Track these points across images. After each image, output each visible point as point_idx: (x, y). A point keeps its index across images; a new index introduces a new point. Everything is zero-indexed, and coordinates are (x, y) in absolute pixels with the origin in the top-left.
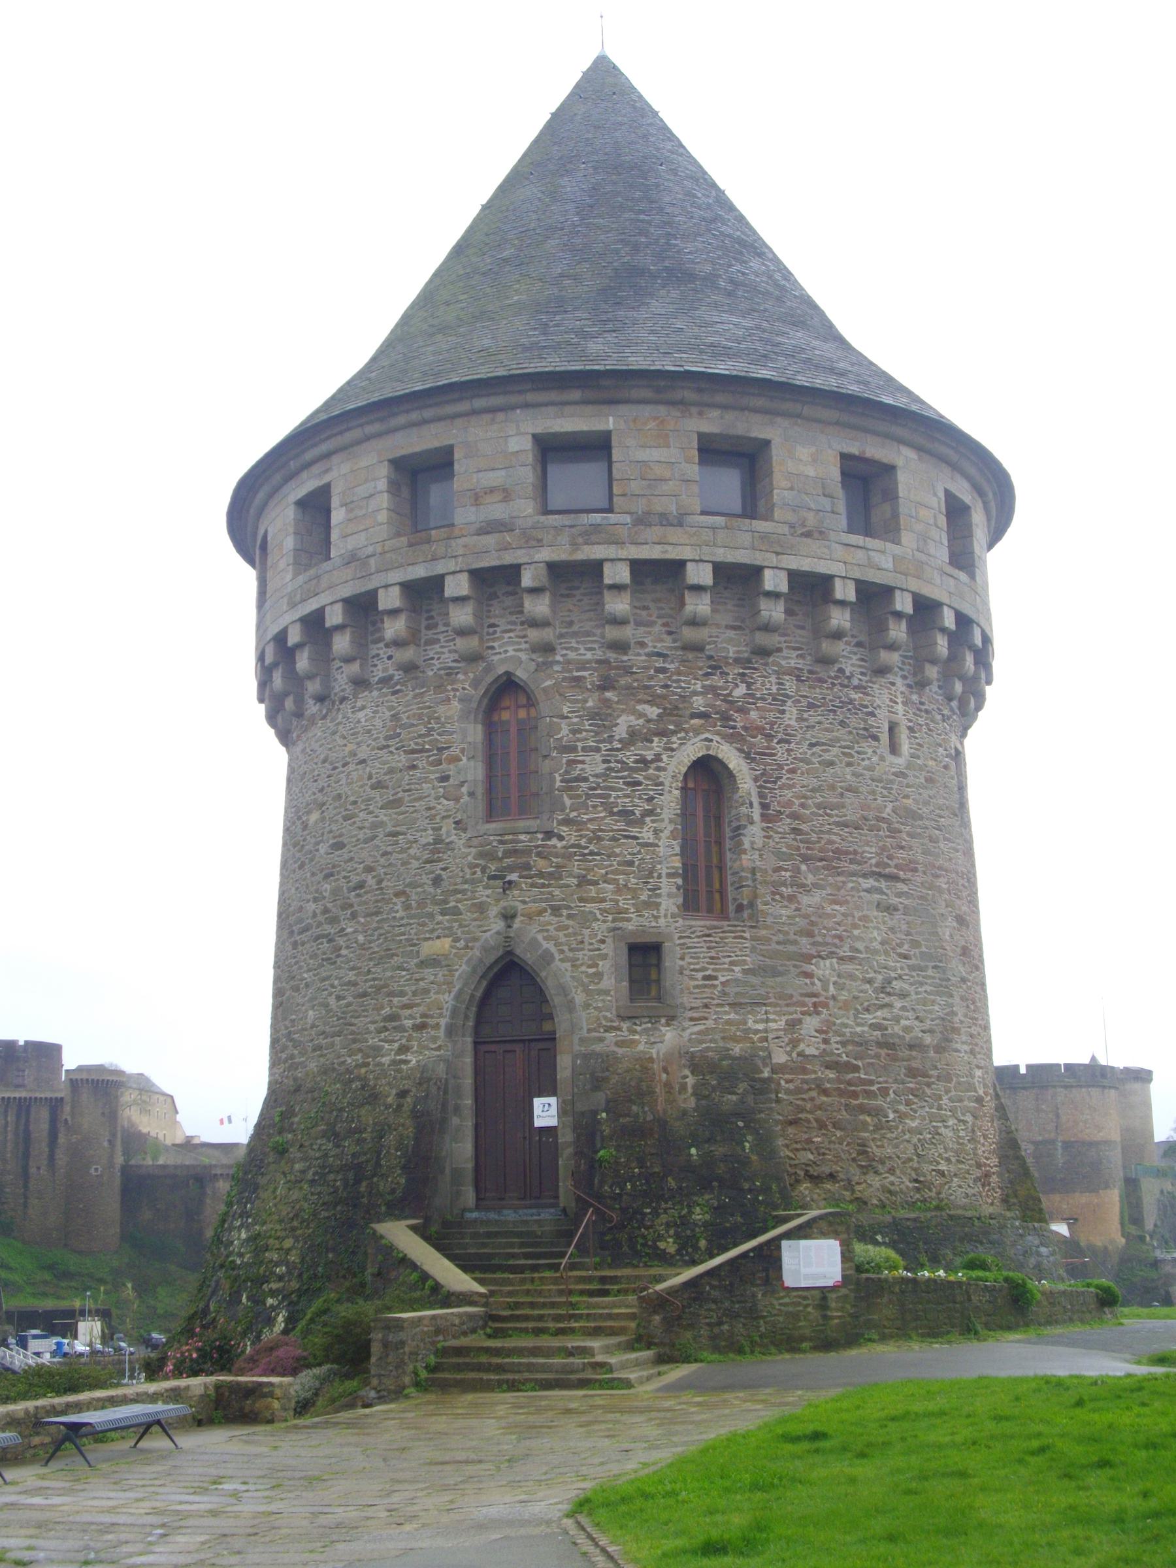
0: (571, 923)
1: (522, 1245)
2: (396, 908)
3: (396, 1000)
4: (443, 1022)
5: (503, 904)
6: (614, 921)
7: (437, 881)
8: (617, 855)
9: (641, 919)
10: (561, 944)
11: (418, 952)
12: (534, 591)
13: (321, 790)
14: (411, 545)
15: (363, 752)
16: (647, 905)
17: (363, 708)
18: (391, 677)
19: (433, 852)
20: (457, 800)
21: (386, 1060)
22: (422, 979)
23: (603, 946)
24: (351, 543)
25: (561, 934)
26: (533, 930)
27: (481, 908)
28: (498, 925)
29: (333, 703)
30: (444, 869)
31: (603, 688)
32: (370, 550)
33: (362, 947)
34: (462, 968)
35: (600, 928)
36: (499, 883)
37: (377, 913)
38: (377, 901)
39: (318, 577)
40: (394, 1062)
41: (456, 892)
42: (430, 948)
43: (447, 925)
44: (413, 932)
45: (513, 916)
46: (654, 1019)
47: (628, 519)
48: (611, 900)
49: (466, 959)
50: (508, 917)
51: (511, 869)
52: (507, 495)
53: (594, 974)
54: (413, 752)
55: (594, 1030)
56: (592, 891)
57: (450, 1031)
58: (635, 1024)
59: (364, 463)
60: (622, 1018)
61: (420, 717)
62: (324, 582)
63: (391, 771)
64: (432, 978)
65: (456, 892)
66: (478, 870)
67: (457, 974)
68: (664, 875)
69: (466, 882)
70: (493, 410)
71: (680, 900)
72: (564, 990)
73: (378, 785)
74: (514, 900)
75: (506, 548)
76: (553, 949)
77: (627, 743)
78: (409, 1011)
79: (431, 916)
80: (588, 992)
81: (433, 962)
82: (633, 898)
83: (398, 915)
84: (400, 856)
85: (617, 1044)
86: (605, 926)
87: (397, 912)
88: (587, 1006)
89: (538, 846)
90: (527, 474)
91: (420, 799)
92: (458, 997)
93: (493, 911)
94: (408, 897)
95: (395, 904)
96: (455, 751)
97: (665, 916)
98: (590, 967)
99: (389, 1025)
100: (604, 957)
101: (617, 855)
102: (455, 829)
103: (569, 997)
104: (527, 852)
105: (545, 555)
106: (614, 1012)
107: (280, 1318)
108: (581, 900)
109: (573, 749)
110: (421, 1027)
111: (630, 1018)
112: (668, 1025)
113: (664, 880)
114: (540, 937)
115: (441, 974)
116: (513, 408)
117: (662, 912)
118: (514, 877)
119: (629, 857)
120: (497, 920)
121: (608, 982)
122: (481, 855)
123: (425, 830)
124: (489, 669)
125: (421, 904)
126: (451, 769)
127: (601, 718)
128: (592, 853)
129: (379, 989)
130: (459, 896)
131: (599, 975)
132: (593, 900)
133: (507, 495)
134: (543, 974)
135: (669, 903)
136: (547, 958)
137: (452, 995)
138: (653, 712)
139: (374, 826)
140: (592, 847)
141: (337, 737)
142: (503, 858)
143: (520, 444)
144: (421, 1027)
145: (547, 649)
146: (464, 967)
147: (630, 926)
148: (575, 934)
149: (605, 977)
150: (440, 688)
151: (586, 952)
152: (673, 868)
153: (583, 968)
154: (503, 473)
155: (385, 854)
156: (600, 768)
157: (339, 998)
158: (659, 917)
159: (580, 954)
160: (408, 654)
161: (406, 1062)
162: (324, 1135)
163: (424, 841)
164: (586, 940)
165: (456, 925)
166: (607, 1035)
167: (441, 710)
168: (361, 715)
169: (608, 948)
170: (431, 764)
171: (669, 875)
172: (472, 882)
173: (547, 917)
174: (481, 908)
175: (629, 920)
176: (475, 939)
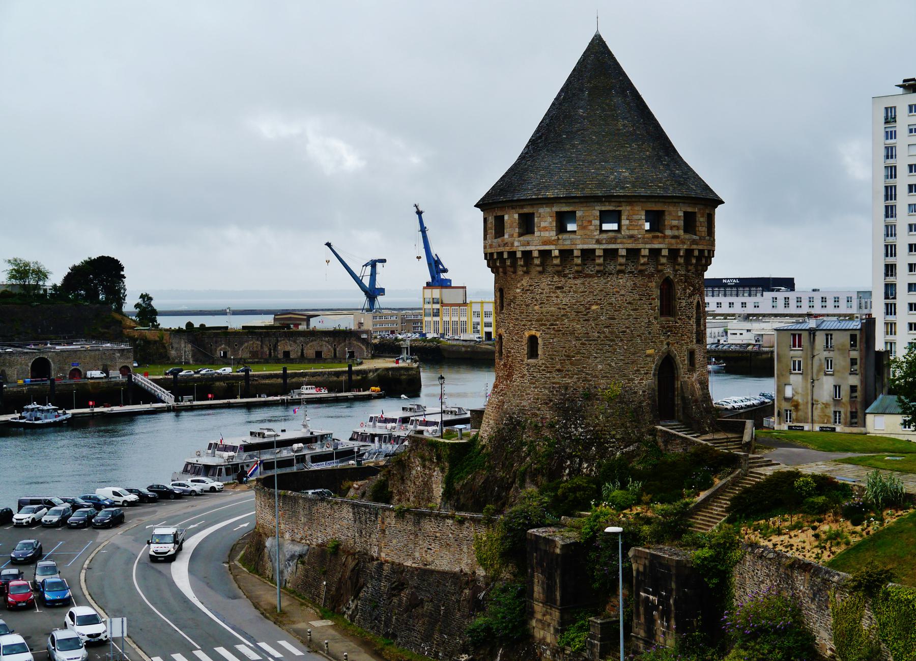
4: (652, 372)
7: (650, 333)
12: (681, 256)
13: (601, 299)
15: (622, 292)
17: (621, 279)
18: (634, 272)
19: (648, 325)
20: (655, 311)
24: (631, 232)
26: (673, 348)
27: (662, 342)
29: (605, 274)
31: (685, 282)
32: (640, 236)
33: (626, 350)
37: (631, 341)
40: (639, 383)
42: (649, 352)
47: (697, 238)
50: (668, 344)
51: (668, 331)
52: (678, 228)
54: (641, 295)
57: (654, 375)
59: (636, 208)
60: (688, 371)
61: (643, 285)
62: (619, 241)
63: (634, 300)
65: (655, 337)
70: (675, 203)
74: (670, 340)
75: (677, 243)
77: (689, 297)
79: (649, 343)
80: (683, 365)
90: (682, 223)
91: (644, 309)
92: (656, 366)
93: (665, 343)
94: (641, 337)
96: (654, 296)
99: (637, 372)
100: (685, 355)
104: (671, 327)
105: (685, 247)
107: (618, 453)
109: (680, 299)
110: (646, 374)
116: (679, 203)
118: (669, 333)
121: (686, 362)
122: (661, 327)
124: (664, 274)
125: (645, 340)
127: (684, 290)
129: (633, 363)
131: (684, 360)
133: (678, 228)
138: (692, 288)
139: (628, 315)
141: (608, 285)
143: (681, 214)
144: (646, 374)
145: (677, 271)
147: (689, 347)
150: (649, 278)
154: (677, 222)
155: (633, 324)
156: (684, 305)
157: (616, 364)
160: (643, 268)
162: (620, 403)
167: (650, 284)
168: (621, 280)
169: (686, 353)
170: (647, 299)
173: (676, 345)
174: (662, 342)
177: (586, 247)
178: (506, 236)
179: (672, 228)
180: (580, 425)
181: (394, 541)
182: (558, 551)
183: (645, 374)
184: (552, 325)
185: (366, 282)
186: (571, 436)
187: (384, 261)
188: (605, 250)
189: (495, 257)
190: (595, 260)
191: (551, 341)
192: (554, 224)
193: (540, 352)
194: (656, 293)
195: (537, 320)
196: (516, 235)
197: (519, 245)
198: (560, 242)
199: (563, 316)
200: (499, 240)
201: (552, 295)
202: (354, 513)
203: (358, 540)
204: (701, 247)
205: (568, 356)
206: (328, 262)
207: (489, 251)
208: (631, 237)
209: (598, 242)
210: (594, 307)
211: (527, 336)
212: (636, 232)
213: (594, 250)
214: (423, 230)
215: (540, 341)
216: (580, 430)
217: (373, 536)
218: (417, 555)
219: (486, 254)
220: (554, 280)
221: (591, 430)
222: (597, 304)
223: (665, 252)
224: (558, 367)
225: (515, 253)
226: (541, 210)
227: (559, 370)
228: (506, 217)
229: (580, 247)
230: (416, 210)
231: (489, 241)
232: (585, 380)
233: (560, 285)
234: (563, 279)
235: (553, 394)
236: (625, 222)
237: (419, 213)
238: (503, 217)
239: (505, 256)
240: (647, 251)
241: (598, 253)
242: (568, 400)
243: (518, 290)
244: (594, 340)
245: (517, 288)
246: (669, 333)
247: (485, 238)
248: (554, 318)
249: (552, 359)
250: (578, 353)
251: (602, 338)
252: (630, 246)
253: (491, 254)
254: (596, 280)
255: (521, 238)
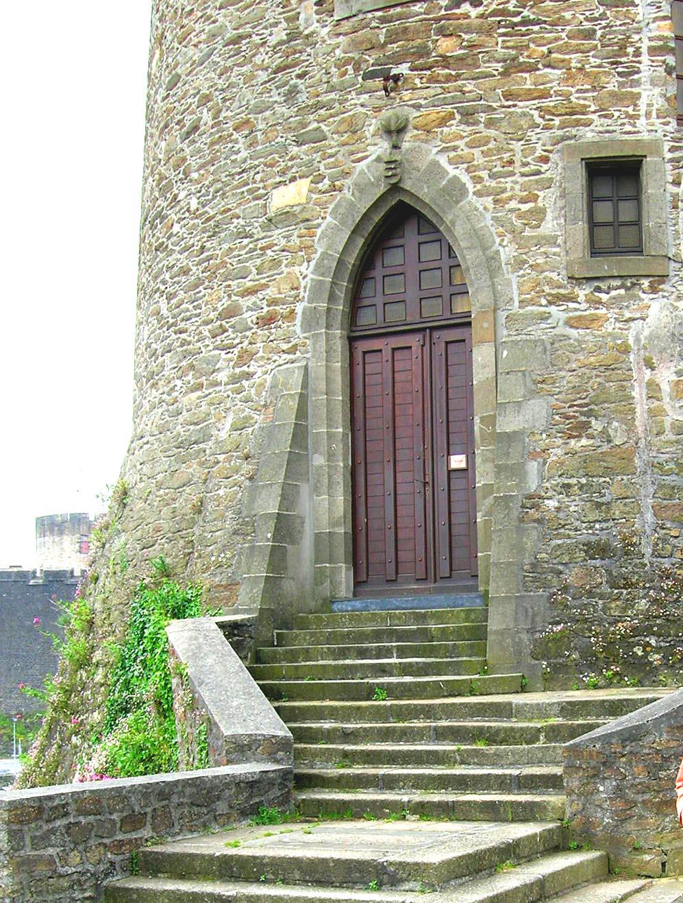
0: (492, 133)
1: (402, 653)
2: (237, 146)
3: (233, 283)
4: (299, 308)
5: (385, 113)
6: (561, 128)
7: (292, 94)
8: (567, 23)
9: (609, 121)
10: (477, 168)
11: (265, 206)
16: (617, 98)
21: (222, 376)
22: (269, 247)
23: (545, 167)
25: (477, 152)
26: (432, 152)
28: (381, 147)
30: (300, 76)
35: (541, 140)
36: (378, 82)
38: (213, 144)
40: (235, 379)
41: (318, 106)
43: (306, 158)
44: (258, 177)
45: (401, 130)
46: (630, 281)
48: (557, 94)
49: (331, 206)
50: (395, 131)
53: (530, 211)
55: (532, 302)
56: (528, 81)
58: (598, 289)
64: (283, 242)
66: (350, 67)
67: (319, 231)
68: (644, 50)
69: (332, 89)
71: (672, 91)
72: (482, 243)
76: (465, 178)
78: (253, 299)
81: (287, 217)
82: (594, 89)
83: (239, 157)
84: (244, 69)
85: (569, 323)
86: (547, 134)
87: (239, 152)
88: (519, 264)
89: (438, 20)
95: (236, 141)
97: (648, 115)
98: (523, 201)
100: (548, 184)
101: (567, 23)
102: (317, 13)
103: (490, 253)
106: (564, 272)
108: (508, 96)
110: (267, 321)
111: (589, 279)
112: (654, 290)
113: (645, 58)
114: (443, 160)
117: (643, 109)
118: (403, 69)
119: (587, 25)
120: (378, 140)
122: (355, 45)
123: (276, 24)
128: (525, 22)
130: (322, 112)
131: (540, 214)
132: (529, 95)
134: (448, 218)
136: (455, 190)
137: (313, 264)
140: (526, 13)
142: (386, 44)
144: (267, 321)
146: (329, 219)
147: (589, 135)
148: (499, 150)
149: (549, 216)
151: (517, 178)
152: (660, 38)
153: (513, 204)
158: (637, 117)
159: (508, 182)
161: (249, 376)
163: (273, 41)
164: (518, 158)
165: (317, 156)
166: (553, 309)
171: (653, 51)
172: (342, 88)
173: (454, 127)
174: (354, 128)
175: (588, 124)
176: (346, 174)
246: (403, 69)
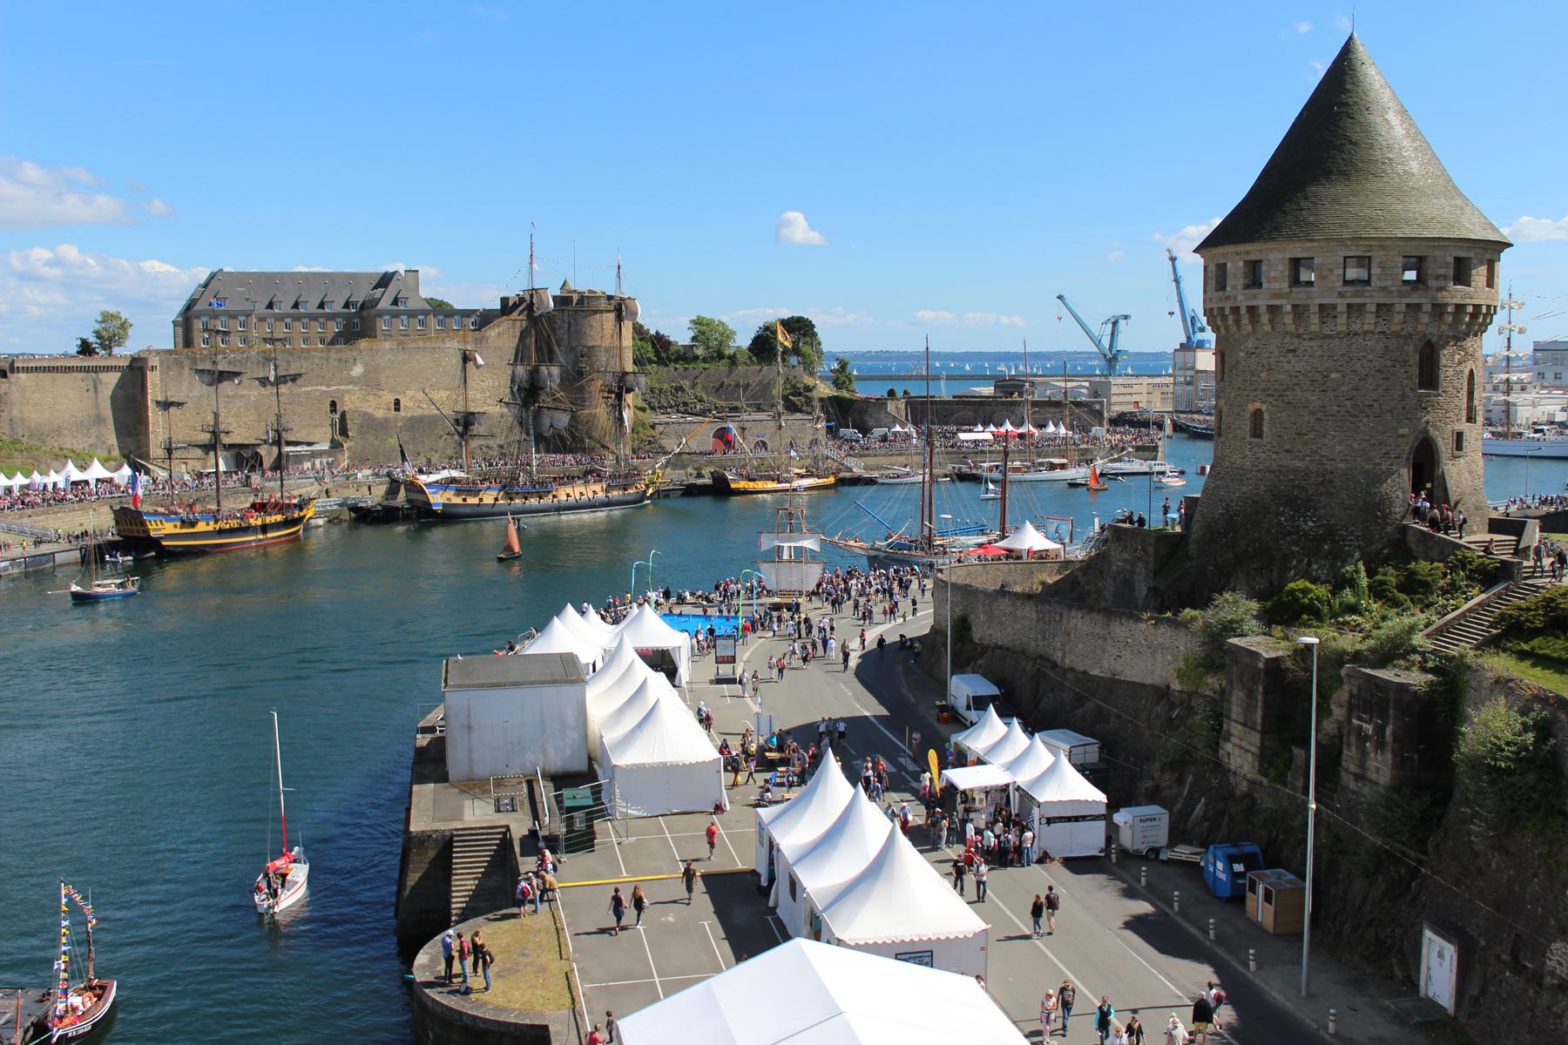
7: (1404, 408)
14: (1412, 290)
15: (1370, 357)
21: (1384, 467)
24: (1384, 284)
32: (1394, 288)
34: (1412, 439)
39: (1363, 291)
42: (1401, 431)
56: (1448, 415)
57: (1408, 459)
62: (1367, 294)
63: (1385, 366)
73: (1379, 371)
81: (1403, 436)
90: (1451, 272)
96: (1411, 363)
115: (1405, 440)
126: (1409, 369)
129: (1380, 443)
135: (1464, 419)
139: (1377, 385)
143: (1451, 260)
167: (1406, 348)
168: (1368, 343)
177: (1324, 301)
178: (1228, 289)
179: (1437, 277)
180: (1311, 517)
181: (1080, 646)
182: (1261, 665)
183: (1396, 458)
184: (1281, 395)
185: (1106, 342)
186: (1298, 532)
187: (1126, 317)
188: (1349, 306)
189: (1215, 313)
190: (1335, 317)
191: (1279, 415)
192: (1287, 273)
193: (1265, 429)
194: (1415, 358)
195: (1263, 390)
196: (1240, 287)
197: (1243, 301)
198: (1294, 295)
199: (1295, 385)
200: (1221, 293)
201: (1282, 359)
202: (1037, 612)
203: (1040, 643)
204: (1476, 302)
205: (1300, 434)
206: (1060, 319)
207: (1209, 306)
208: (1384, 289)
209: (1341, 295)
210: (1334, 376)
211: (1251, 407)
212: (1389, 283)
213: (1334, 307)
214: (1177, 281)
215: (1266, 416)
216: (1310, 524)
217: (1057, 639)
218: (1105, 663)
219: (1205, 310)
220: (1286, 341)
221: (1324, 525)
222: (1338, 371)
223: (1427, 308)
224: (1287, 447)
225: (1238, 308)
226: (1271, 257)
227: (1287, 451)
228: (1229, 265)
229: (1318, 301)
230: (1167, 255)
231: (1209, 295)
232: (1320, 463)
233: (1292, 348)
234: (1296, 341)
235: (1279, 480)
236: (1375, 271)
237: (1173, 259)
238: (1225, 265)
239: (1227, 312)
240: (1404, 307)
241: (1339, 309)
242: (1297, 487)
243: (1241, 354)
244: (1333, 415)
245: (1241, 350)
247: (1205, 292)
248: (1284, 387)
249: (1279, 436)
250: (1314, 430)
251: (1343, 413)
252: (1382, 301)
253: (1211, 310)
254: (1337, 342)
255: (1247, 291)
